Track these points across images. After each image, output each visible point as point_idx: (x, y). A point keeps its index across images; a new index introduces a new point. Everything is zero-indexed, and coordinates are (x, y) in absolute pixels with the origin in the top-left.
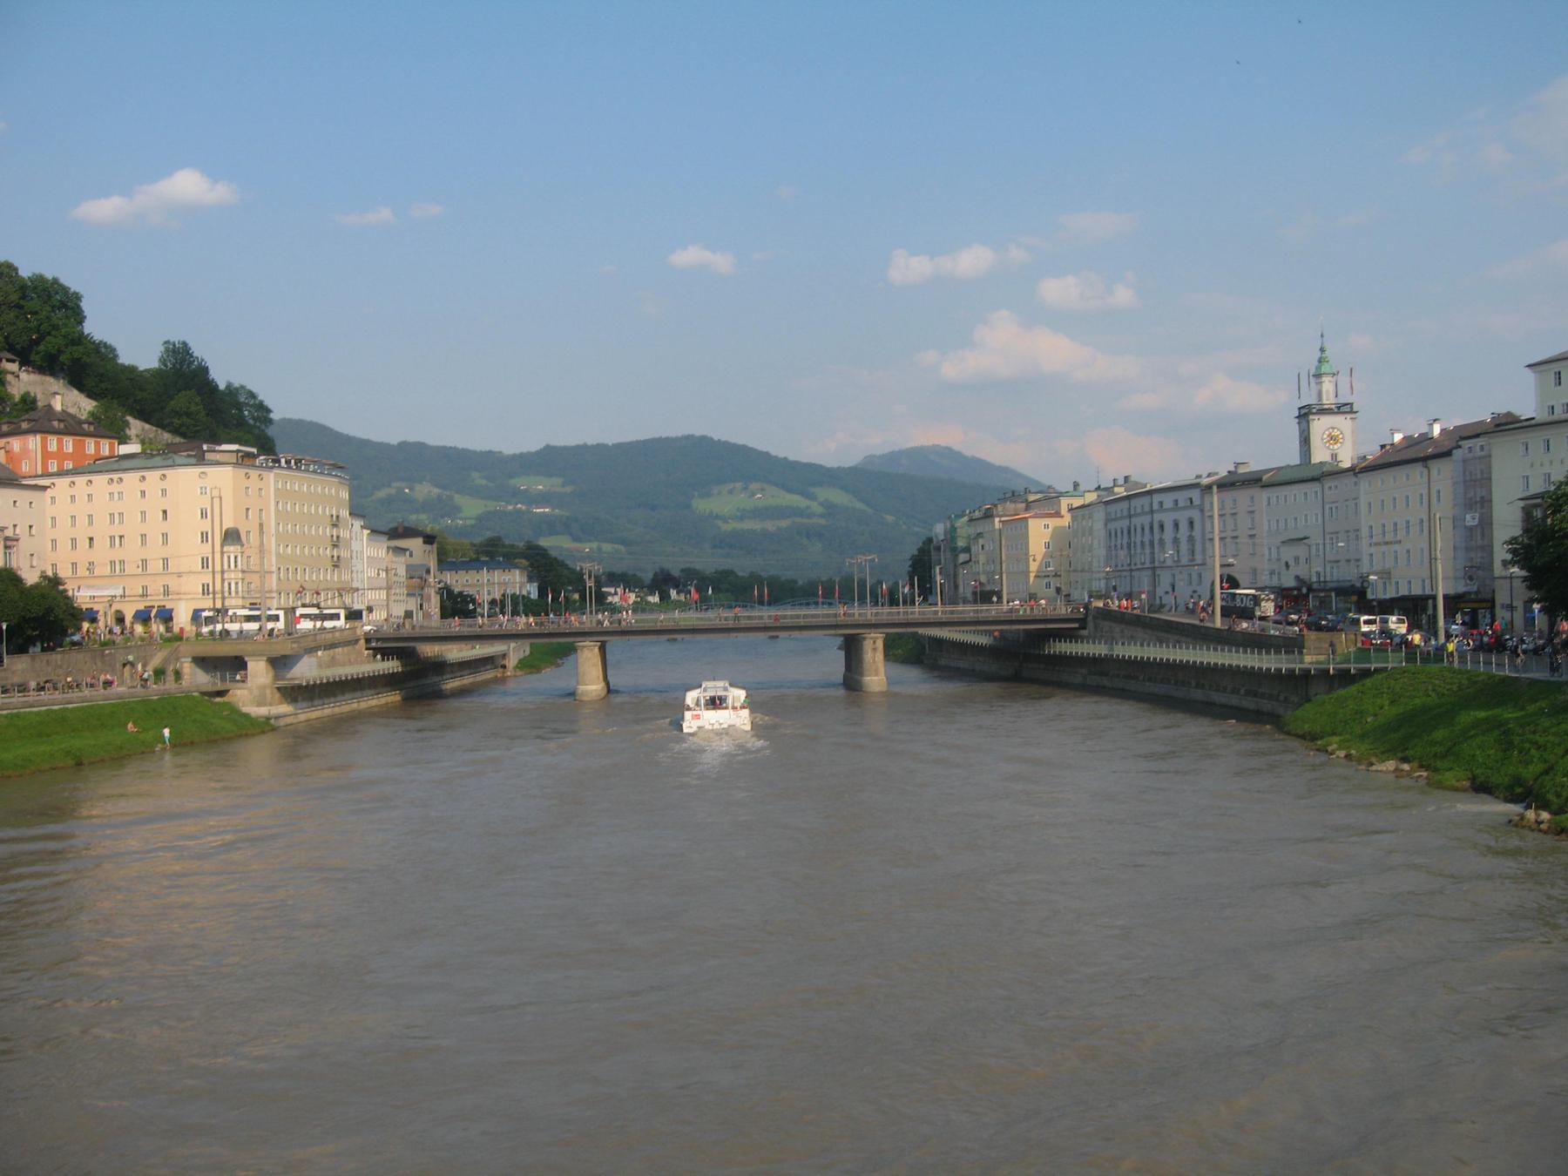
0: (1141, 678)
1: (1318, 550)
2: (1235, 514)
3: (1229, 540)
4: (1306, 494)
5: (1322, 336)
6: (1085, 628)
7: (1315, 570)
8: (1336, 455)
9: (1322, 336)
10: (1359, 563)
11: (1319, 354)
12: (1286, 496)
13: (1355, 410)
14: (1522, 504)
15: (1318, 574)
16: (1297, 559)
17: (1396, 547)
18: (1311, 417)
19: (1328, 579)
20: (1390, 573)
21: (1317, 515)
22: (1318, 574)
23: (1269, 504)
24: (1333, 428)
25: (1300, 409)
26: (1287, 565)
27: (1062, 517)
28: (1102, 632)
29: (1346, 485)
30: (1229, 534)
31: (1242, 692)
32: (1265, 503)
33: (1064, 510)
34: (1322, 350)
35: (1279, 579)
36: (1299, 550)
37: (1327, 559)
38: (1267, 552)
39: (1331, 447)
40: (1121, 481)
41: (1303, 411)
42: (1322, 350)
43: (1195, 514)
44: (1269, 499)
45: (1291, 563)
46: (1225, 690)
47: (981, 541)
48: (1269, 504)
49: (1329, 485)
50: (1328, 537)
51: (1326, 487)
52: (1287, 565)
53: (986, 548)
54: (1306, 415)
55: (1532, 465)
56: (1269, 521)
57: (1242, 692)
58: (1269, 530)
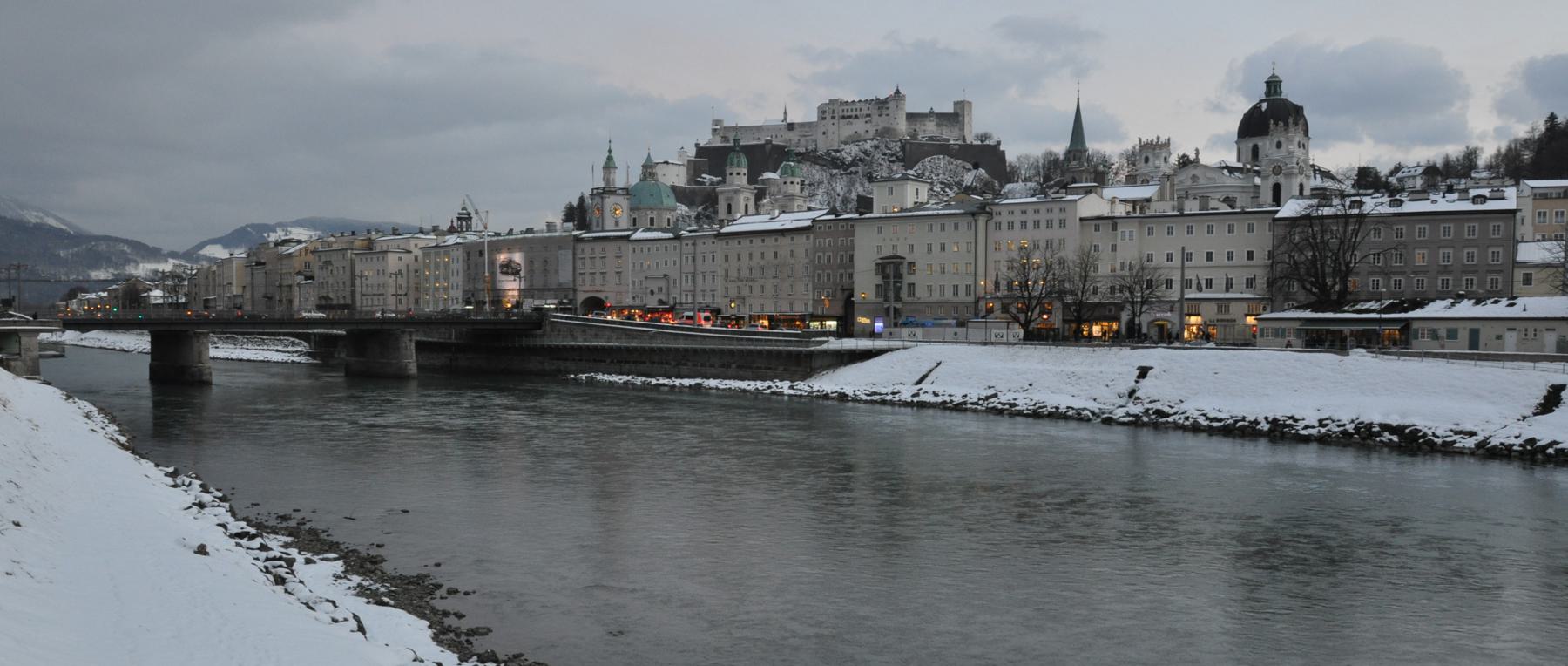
0: (608, 361)
1: (675, 283)
2: (604, 257)
3: (598, 274)
4: (666, 247)
5: (610, 142)
6: (540, 329)
7: (673, 296)
9: (610, 142)
10: (715, 293)
11: (608, 154)
12: (649, 249)
14: (880, 261)
15: (675, 298)
16: (660, 289)
17: (751, 284)
18: (605, 195)
19: (684, 301)
20: (744, 299)
21: (675, 261)
22: (675, 298)
23: (634, 251)
24: (617, 204)
25: (593, 189)
26: (652, 292)
27: (409, 252)
28: (559, 331)
29: (704, 243)
30: (598, 271)
31: (734, 366)
32: (631, 250)
33: (412, 248)
34: (610, 151)
35: (642, 301)
36: (662, 284)
37: (683, 288)
38: (631, 286)
40: (1042, 244)
41: (595, 191)
42: (610, 151)
44: (634, 249)
45: (656, 290)
46: (712, 366)
47: (330, 268)
48: (634, 251)
49: (687, 242)
50: (684, 275)
51: (684, 246)
53: (335, 272)
54: (598, 194)
55: (884, 240)
56: (634, 264)
57: (734, 366)
58: (633, 270)
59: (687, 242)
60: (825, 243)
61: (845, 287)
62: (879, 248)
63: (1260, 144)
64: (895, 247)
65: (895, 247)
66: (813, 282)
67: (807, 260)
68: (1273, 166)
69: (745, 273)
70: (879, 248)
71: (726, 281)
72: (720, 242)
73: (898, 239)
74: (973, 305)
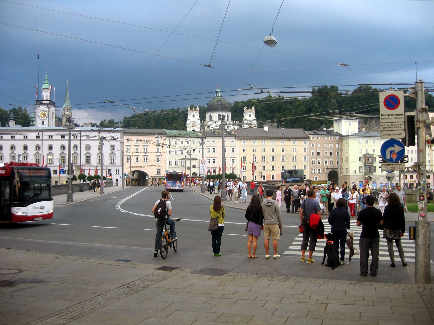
8: (44, 122)
13: (56, 106)
39: (42, 118)
43: (117, 145)
49: (209, 140)
55: (363, 146)
59: (209, 140)
60: (316, 146)
61: (328, 168)
62: (360, 150)
63: (212, 115)
64: (367, 150)
65: (367, 150)
66: (310, 164)
67: (305, 154)
68: (193, 123)
70: (360, 150)
72: (238, 142)
73: (368, 146)
74: (399, 176)
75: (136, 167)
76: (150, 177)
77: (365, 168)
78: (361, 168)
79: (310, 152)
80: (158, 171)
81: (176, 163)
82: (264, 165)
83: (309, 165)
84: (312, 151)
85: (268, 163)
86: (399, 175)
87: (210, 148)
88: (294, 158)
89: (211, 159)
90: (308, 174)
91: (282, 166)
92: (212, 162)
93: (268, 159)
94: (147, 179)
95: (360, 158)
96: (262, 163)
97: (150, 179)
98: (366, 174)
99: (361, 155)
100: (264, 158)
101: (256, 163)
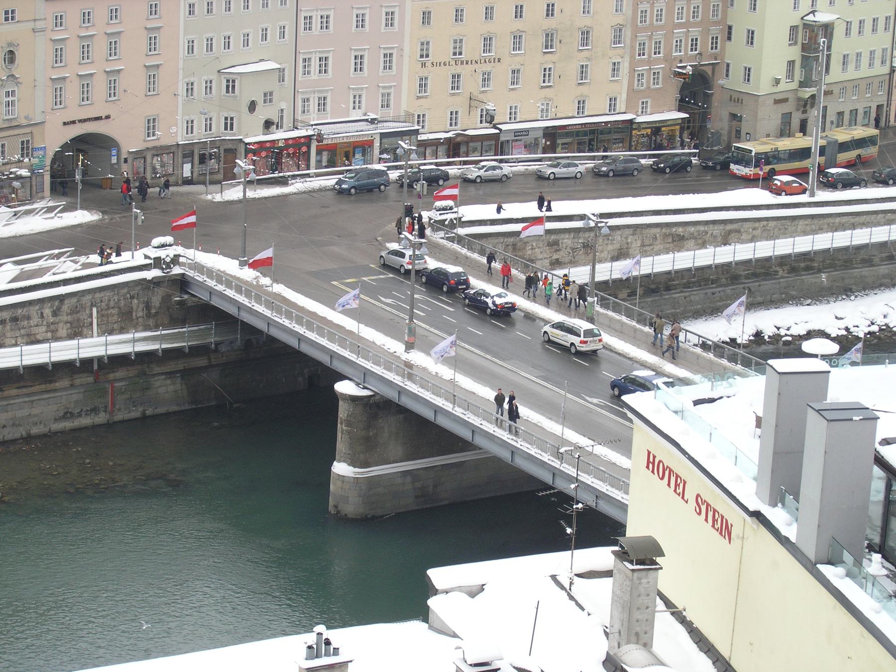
38: (182, 90)
52: (252, 106)
67: (619, 19)
69: (472, 49)
71: (424, 65)
75: (85, 121)
76: (124, 155)
77: (803, 66)
78: (791, 63)
79: (635, 11)
80: (151, 125)
81: (209, 88)
82: (487, 68)
83: (627, 59)
84: (642, 7)
85: (499, 61)
86: (890, 74)
87: (314, 14)
88: (586, 35)
89: (313, 56)
90: (620, 94)
91: (545, 69)
92: (318, 68)
93: (502, 46)
94: (114, 160)
95: (794, 29)
96: (483, 61)
97: (126, 161)
98: (802, 84)
99: (796, 22)
100: (488, 42)
101: (462, 63)
